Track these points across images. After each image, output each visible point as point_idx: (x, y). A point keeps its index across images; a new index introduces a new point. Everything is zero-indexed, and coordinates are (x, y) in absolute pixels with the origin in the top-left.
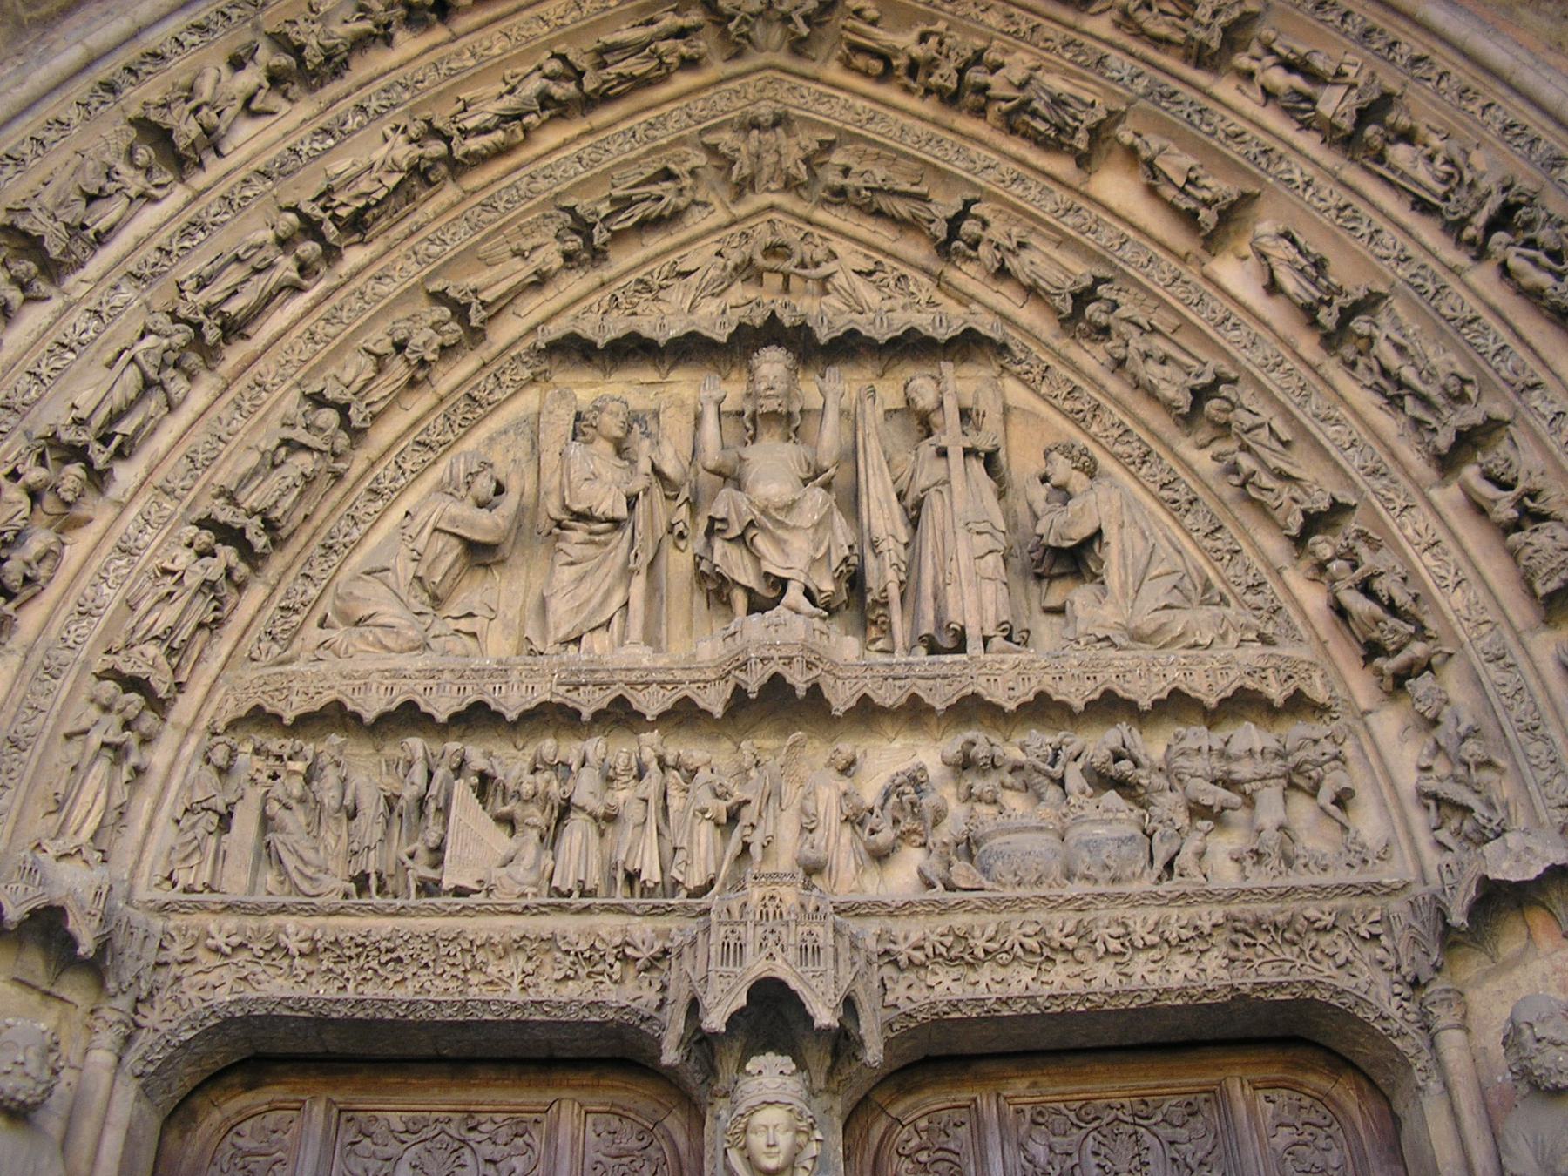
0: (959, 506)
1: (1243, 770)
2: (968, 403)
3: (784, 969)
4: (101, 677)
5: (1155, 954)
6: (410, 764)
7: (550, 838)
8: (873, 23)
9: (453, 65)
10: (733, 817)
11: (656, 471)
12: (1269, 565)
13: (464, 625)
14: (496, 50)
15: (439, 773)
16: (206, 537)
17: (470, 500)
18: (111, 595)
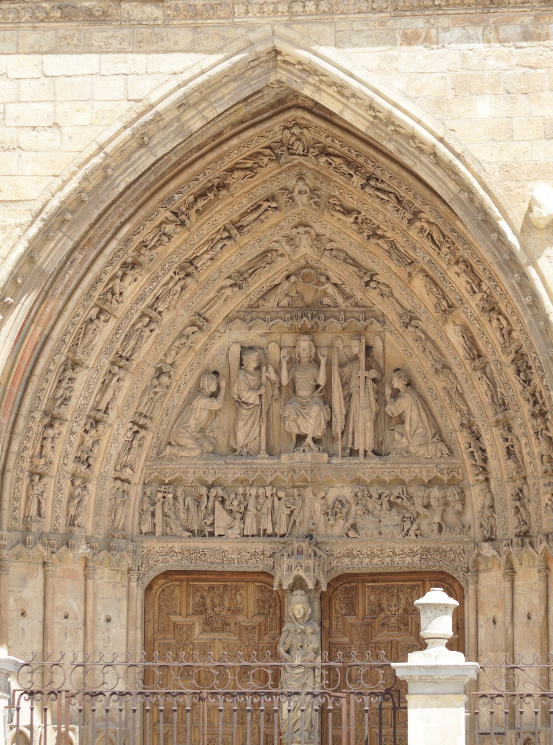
0: (361, 402)
1: (433, 502)
2: (371, 343)
3: (302, 573)
4: (116, 479)
5: (401, 556)
6: (202, 495)
7: (243, 519)
8: (339, 211)
9: (192, 242)
10: (292, 512)
11: (268, 379)
12: (454, 429)
13: (211, 434)
14: (205, 232)
15: (211, 499)
16: (136, 428)
17: (210, 393)
18: (114, 453)
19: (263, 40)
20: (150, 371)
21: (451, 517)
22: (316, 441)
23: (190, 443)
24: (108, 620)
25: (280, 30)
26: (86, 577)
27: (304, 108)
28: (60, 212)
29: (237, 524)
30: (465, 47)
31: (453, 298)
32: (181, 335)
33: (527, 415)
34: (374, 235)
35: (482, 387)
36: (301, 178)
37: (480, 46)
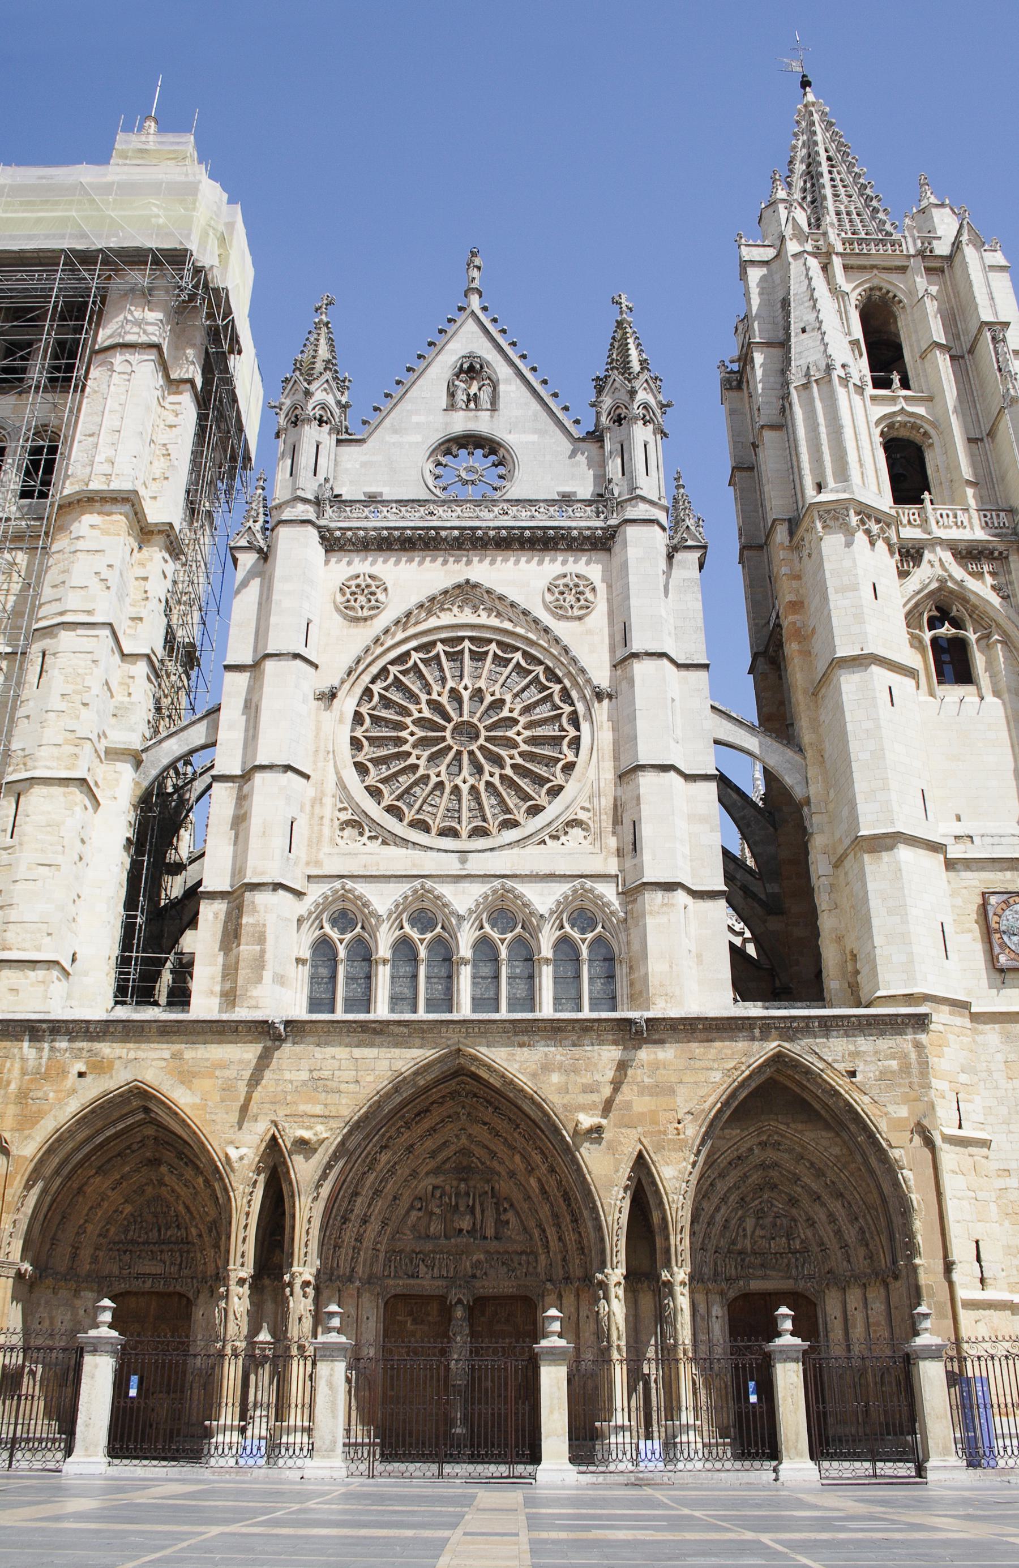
3: (461, 1296)
19: (454, 1044)
20: (391, 1197)
21: (531, 1269)
22: (468, 1232)
23: (408, 1232)
24: (368, 1318)
25: (462, 1040)
26: (358, 1297)
27: (467, 1075)
28: (358, 1122)
29: (430, 1272)
30: (546, 1049)
31: (533, 1165)
32: (405, 1181)
33: (568, 1221)
34: (497, 1134)
35: (547, 1207)
36: (463, 1107)
37: (553, 1049)
